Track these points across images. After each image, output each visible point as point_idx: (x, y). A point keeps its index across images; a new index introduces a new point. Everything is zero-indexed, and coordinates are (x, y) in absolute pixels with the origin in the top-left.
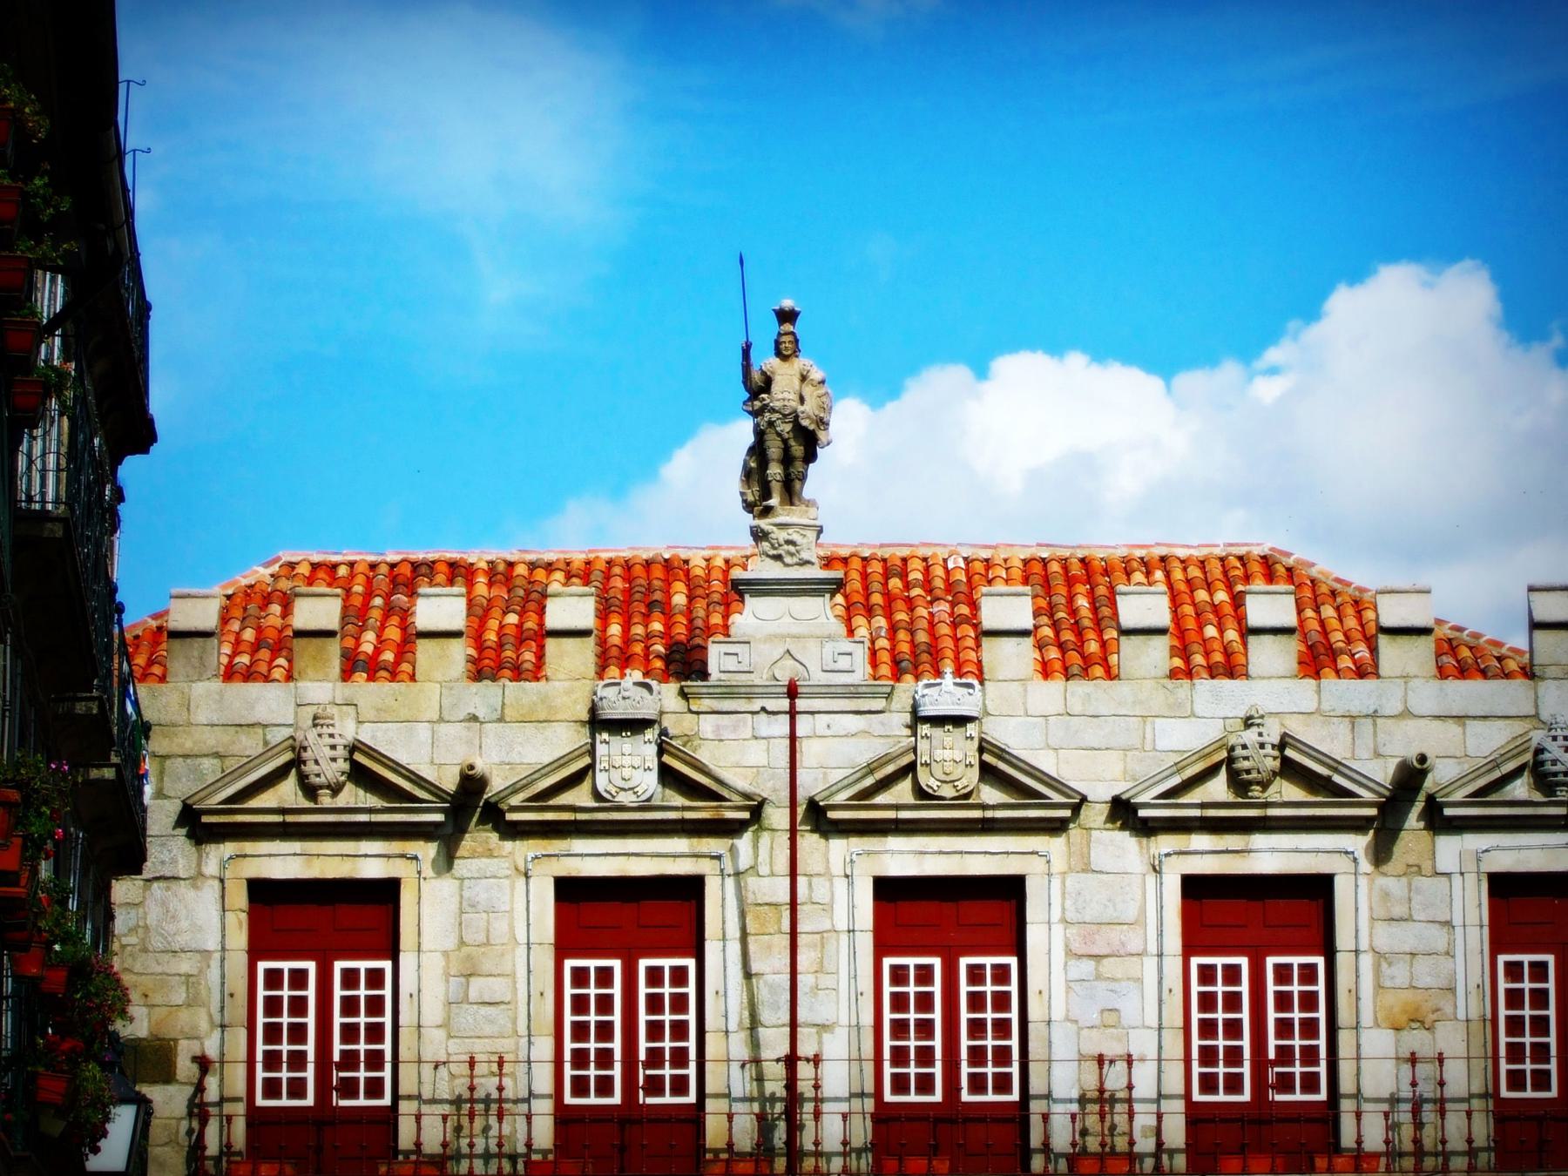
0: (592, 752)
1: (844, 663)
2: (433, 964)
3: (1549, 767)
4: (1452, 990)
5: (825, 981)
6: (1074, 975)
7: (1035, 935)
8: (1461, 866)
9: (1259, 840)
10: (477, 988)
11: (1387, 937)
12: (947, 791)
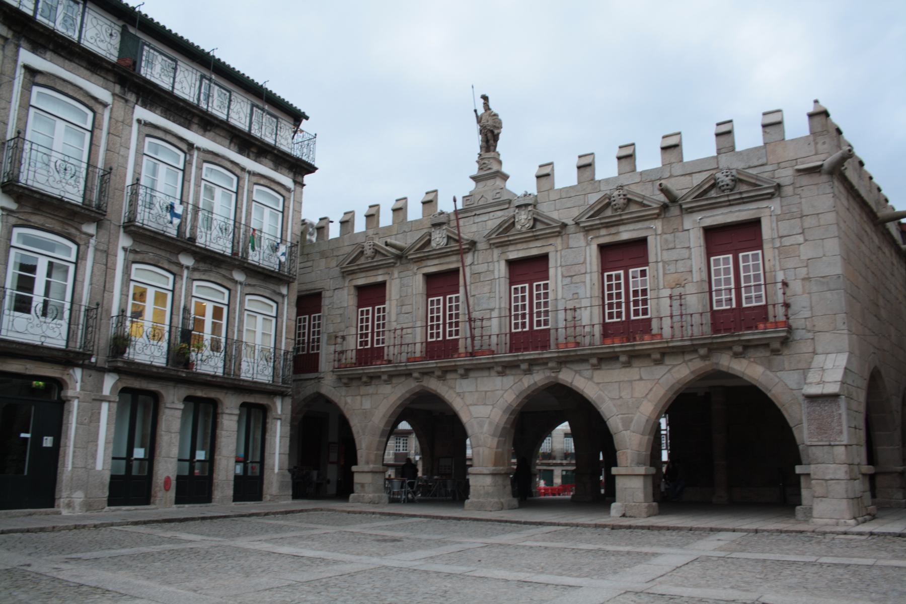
0: (430, 235)
1: (498, 196)
2: (394, 303)
3: (721, 184)
4: (691, 271)
5: (493, 295)
6: (565, 283)
7: (552, 272)
8: (693, 227)
9: (622, 228)
10: (406, 309)
11: (667, 256)
12: (524, 230)
